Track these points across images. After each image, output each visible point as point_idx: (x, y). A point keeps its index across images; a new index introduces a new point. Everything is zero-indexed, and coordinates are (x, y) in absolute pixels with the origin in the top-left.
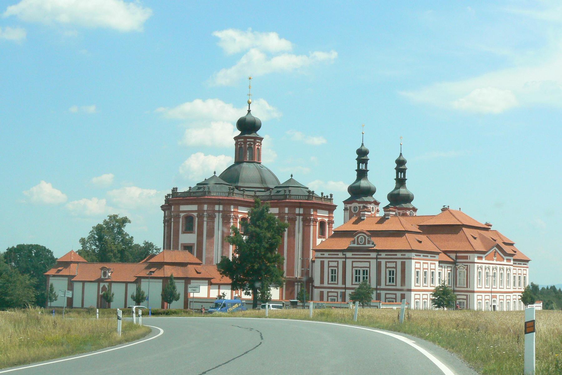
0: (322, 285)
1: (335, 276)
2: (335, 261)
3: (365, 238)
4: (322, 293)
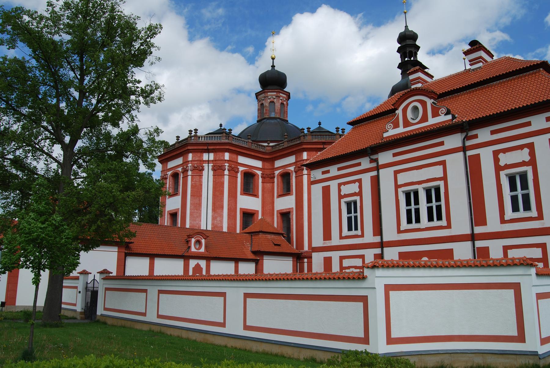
0: (328, 244)
1: (356, 217)
2: (354, 182)
3: (424, 103)
4: (328, 262)
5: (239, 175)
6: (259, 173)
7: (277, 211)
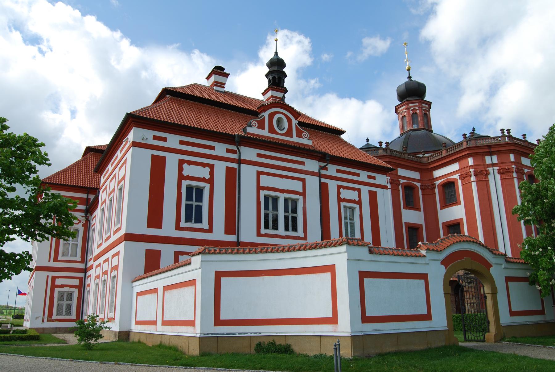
5: (400, 187)
6: (418, 184)
7: (442, 223)
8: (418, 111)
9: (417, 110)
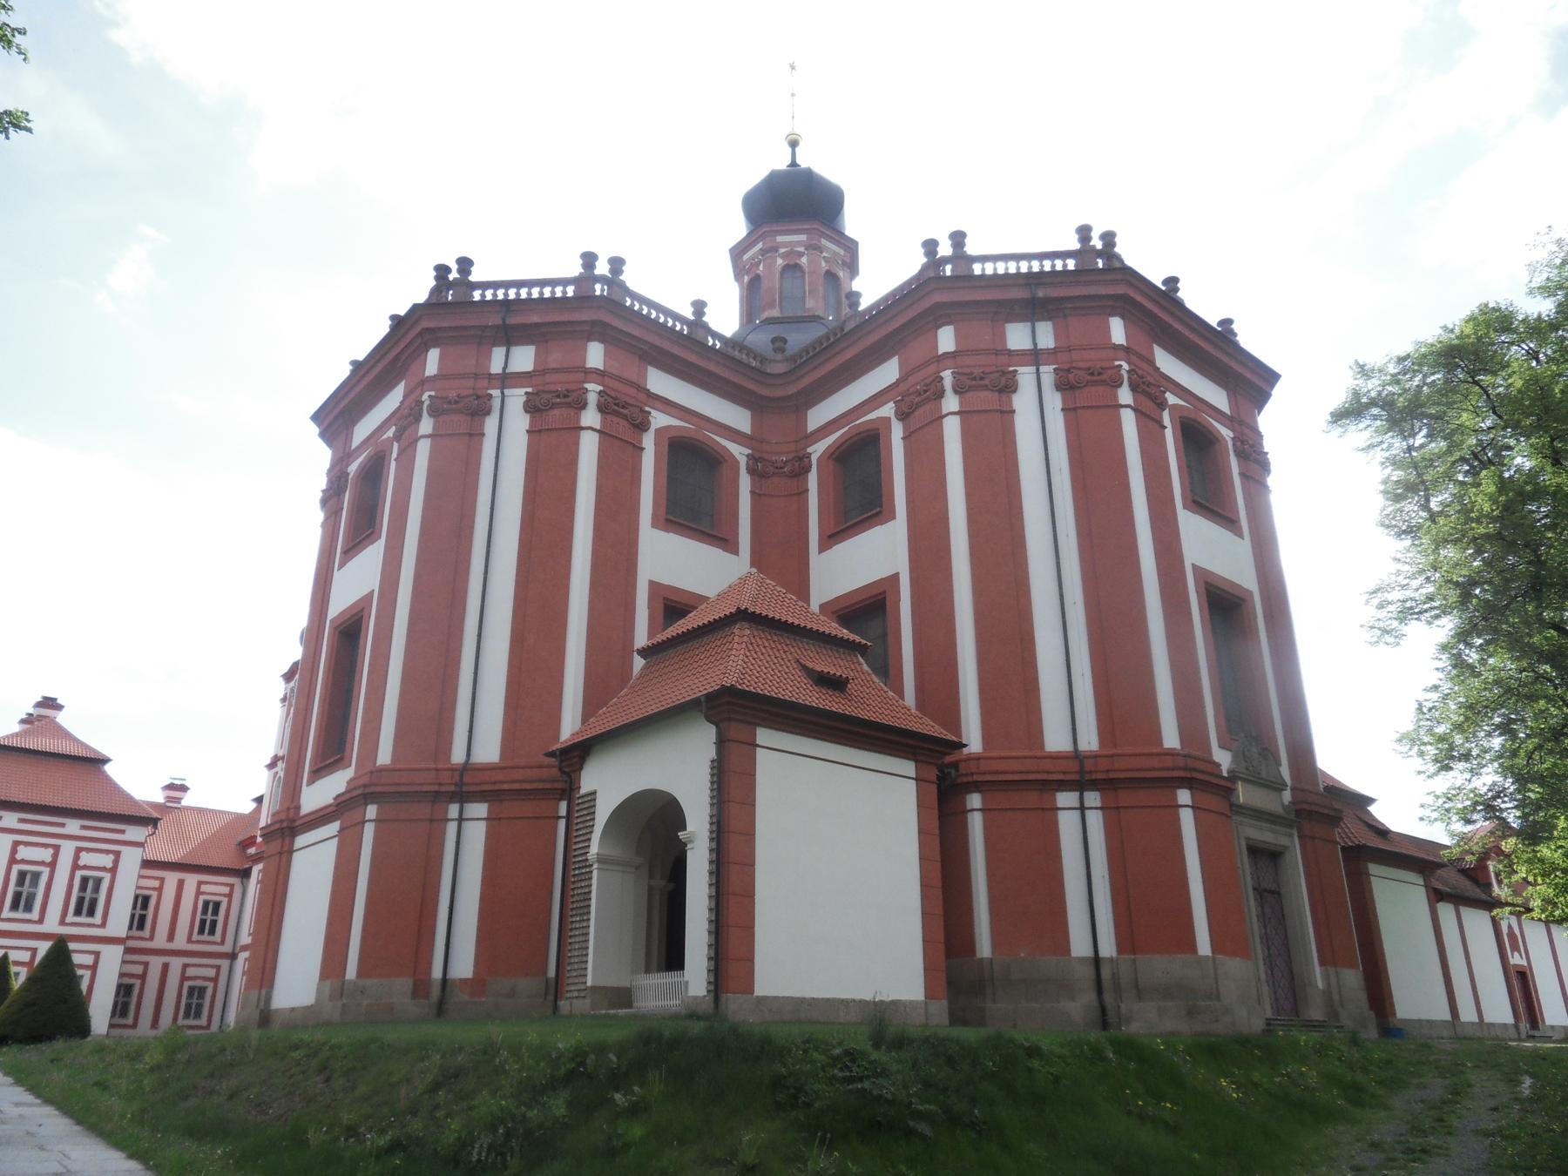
6: (739, 452)
8: (804, 260)
9: (801, 255)
